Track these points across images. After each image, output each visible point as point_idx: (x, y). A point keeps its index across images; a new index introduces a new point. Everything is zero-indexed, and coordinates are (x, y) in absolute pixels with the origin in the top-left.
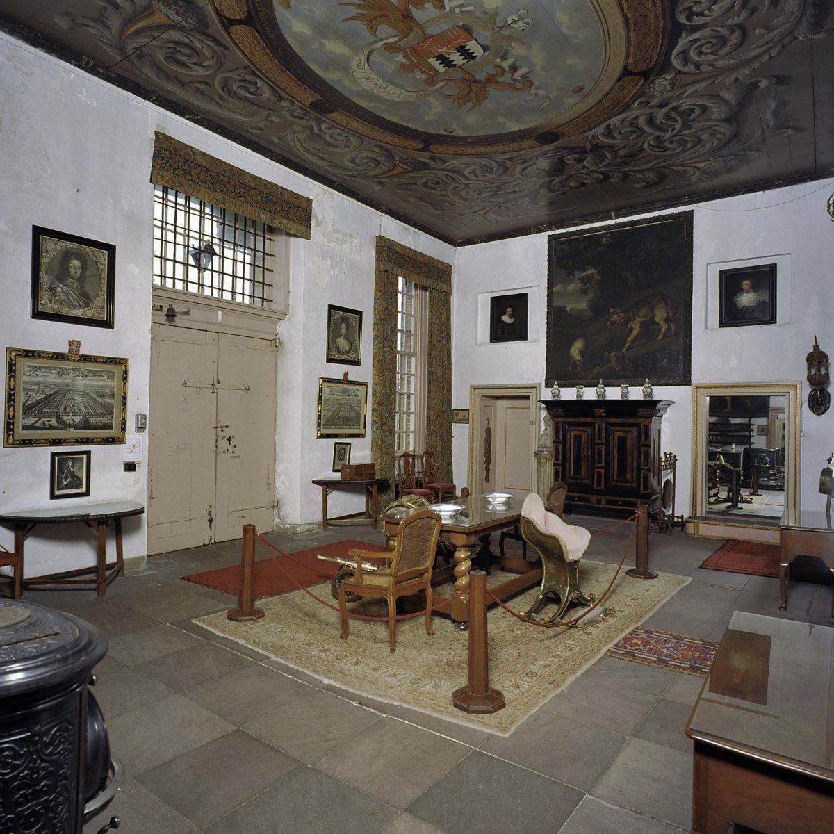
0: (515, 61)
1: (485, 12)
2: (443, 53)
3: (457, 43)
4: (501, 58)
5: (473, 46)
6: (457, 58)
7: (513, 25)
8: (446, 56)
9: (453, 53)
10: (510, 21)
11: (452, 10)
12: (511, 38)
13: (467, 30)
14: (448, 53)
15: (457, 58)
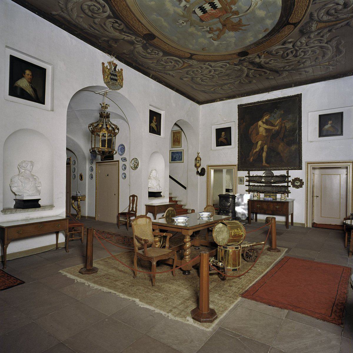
0: (180, 4)
1: (195, 26)
2: (213, 10)
3: (207, 15)
4: (187, 7)
5: (199, 13)
6: (207, 7)
7: (183, 22)
8: (212, 9)
9: (209, 10)
10: (185, 23)
11: (207, 27)
12: (183, 16)
13: (202, 20)
14: (211, 10)
15: (207, 7)
